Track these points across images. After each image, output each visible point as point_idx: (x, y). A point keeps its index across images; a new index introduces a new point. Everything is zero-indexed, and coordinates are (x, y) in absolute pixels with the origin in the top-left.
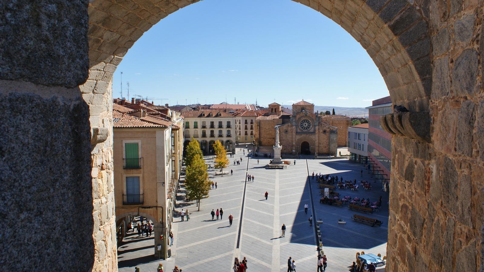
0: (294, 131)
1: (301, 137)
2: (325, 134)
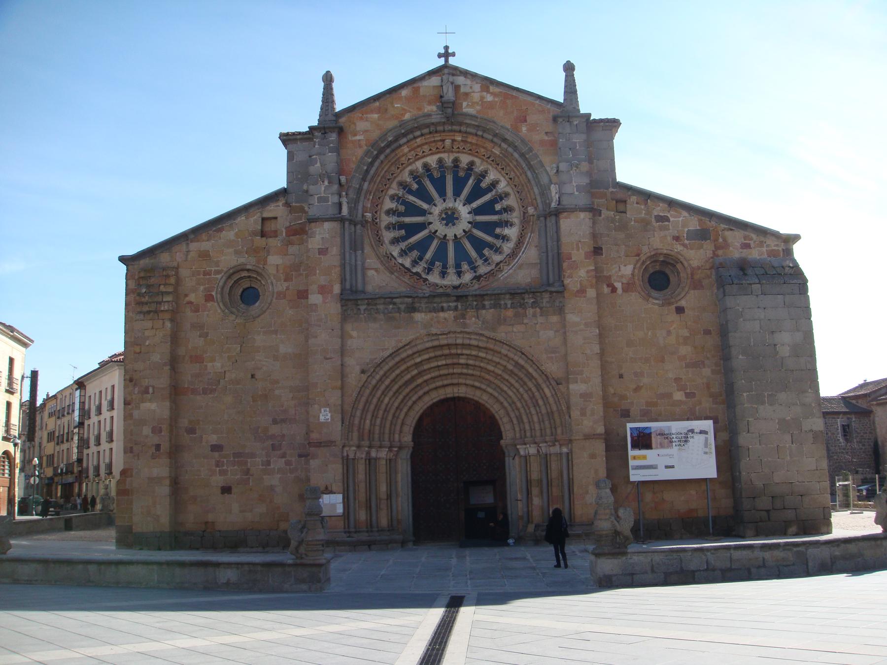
0: (327, 273)
1: (406, 335)
2: (667, 303)
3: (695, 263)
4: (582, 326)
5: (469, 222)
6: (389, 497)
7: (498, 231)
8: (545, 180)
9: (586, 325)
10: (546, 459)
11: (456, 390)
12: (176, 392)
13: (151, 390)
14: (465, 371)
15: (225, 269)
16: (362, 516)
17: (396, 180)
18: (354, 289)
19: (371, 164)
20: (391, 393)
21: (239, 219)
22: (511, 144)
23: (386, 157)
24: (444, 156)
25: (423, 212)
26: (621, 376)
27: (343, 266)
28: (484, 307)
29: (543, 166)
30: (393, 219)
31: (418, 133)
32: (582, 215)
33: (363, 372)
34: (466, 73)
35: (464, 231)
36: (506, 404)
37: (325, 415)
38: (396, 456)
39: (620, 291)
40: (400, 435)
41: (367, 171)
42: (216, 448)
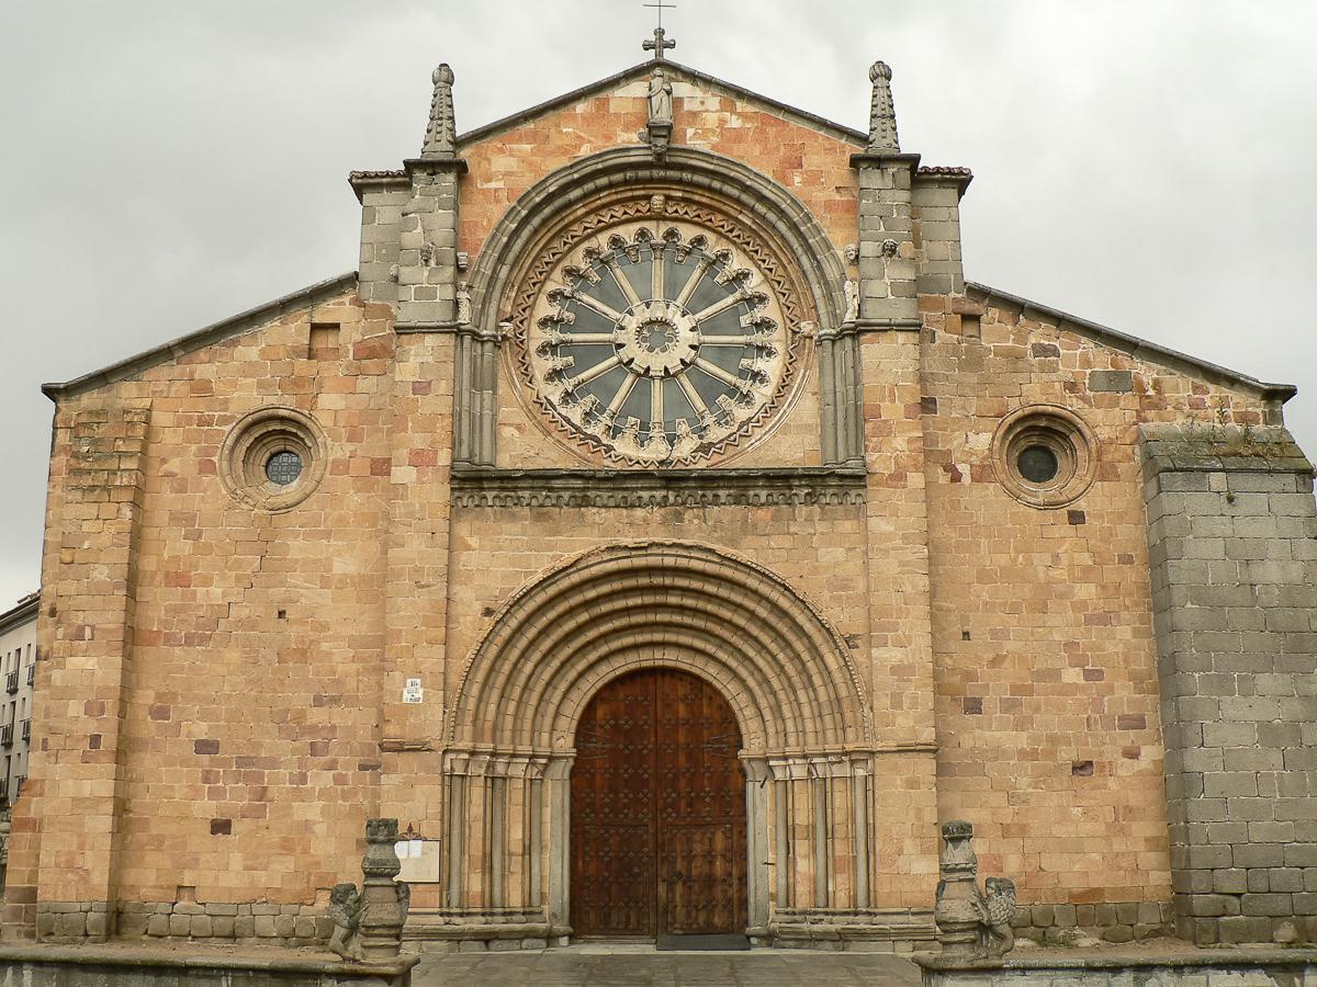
3: (1104, 433)
4: (898, 542)
5: (693, 347)
6: (527, 851)
7: (745, 362)
8: (832, 273)
9: (904, 537)
10: (823, 786)
11: (658, 654)
12: (132, 638)
13: (88, 632)
14: (677, 618)
15: (240, 417)
16: (475, 884)
17: (561, 265)
18: (477, 460)
19: (516, 233)
20: (537, 656)
21: (268, 324)
22: (773, 206)
23: (544, 222)
24: (650, 226)
25: (607, 325)
26: (966, 635)
27: (456, 416)
28: (716, 501)
29: (829, 248)
30: (553, 336)
31: (603, 181)
32: (901, 337)
33: (488, 612)
34: (693, 77)
35: (682, 361)
36: (751, 682)
37: (413, 692)
38: (543, 773)
39: (966, 479)
40: (551, 734)
41: (507, 246)
42: (204, 747)
